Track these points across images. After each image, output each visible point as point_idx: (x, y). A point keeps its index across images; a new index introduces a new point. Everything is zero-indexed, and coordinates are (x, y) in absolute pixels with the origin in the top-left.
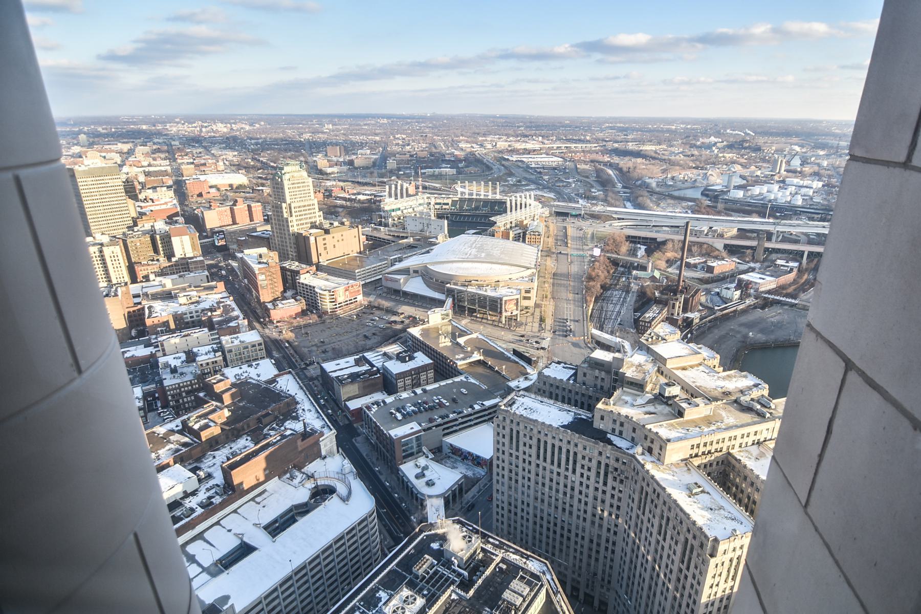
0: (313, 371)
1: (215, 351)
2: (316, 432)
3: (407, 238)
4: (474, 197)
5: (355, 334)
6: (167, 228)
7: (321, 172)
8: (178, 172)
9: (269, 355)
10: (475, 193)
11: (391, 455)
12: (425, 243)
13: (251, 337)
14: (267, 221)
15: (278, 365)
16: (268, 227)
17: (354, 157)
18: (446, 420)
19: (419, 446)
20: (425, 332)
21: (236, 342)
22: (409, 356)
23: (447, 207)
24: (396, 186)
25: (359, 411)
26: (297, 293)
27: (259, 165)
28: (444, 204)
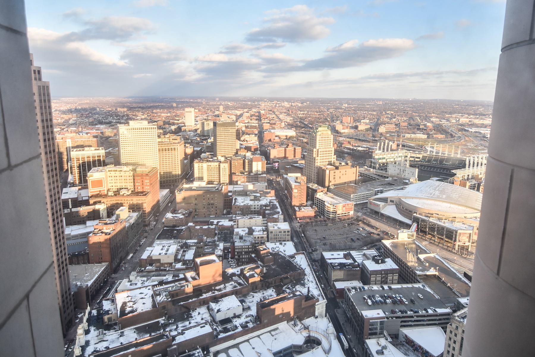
0: (316, 256)
1: (264, 231)
2: (314, 298)
3: (388, 177)
4: (440, 154)
5: (345, 236)
6: (252, 157)
7: (337, 132)
8: (261, 127)
9: (292, 240)
10: (441, 152)
11: (361, 330)
12: (401, 182)
13: (285, 226)
14: (303, 157)
15: (296, 246)
16: (303, 162)
17: (358, 124)
18: (405, 315)
19: (382, 329)
20: (395, 246)
21: (276, 228)
22: (382, 260)
23: (418, 160)
24: (384, 143)
25: (343, 290)
26: (313, 204)
27: (303, 125)
28: (417, 158)
